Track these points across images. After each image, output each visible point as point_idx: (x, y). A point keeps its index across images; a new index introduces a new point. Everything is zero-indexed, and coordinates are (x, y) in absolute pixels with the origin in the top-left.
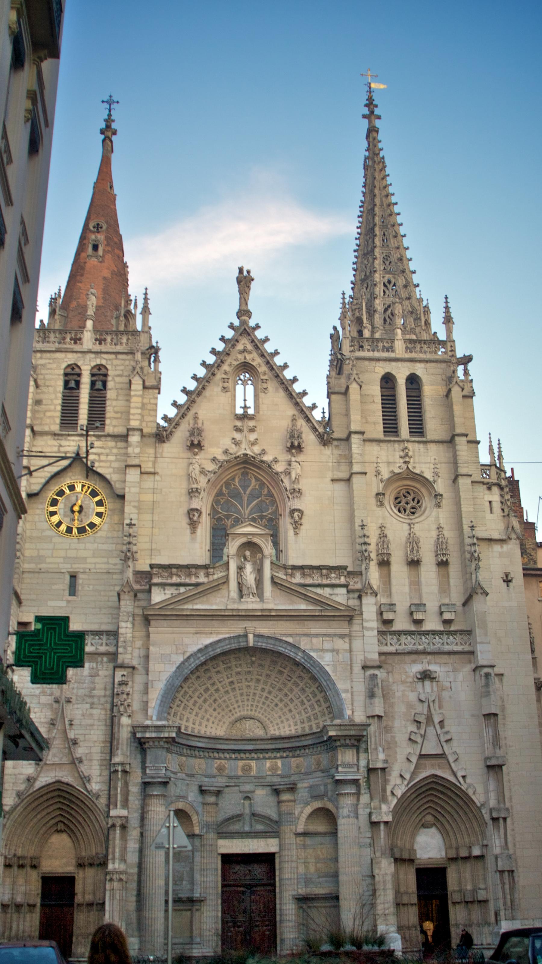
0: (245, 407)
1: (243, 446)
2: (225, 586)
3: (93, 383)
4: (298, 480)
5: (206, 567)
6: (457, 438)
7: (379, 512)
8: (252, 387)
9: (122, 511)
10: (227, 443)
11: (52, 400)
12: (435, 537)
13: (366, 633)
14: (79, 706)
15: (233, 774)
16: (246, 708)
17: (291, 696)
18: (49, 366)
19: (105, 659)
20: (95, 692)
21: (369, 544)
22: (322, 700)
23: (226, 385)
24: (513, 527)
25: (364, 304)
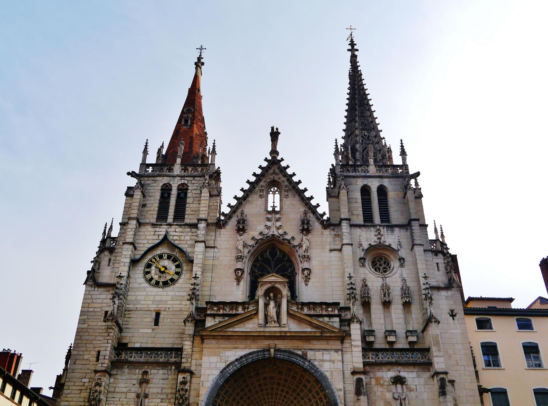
0: (274, 207)
1: (272, 230)
2: (256, 316)
3: (179, 195)
4: (307, 250)
5: (243, 304)
6: (413, 223)
7: (362, 270)
8: (279, 195)
9: (192, 271)
10: (261, 228)
11: (152, 204)
12: (401, 286)
13: (354, 349)
14: (153, 400)
17: (302, 395)
18: (152, 185)
19: (173, 367)
20: (164, 391)
21: (355, 289)
22: (323, 397)
23: (261, 194)
24: (454, 279)
25: (349, 147)
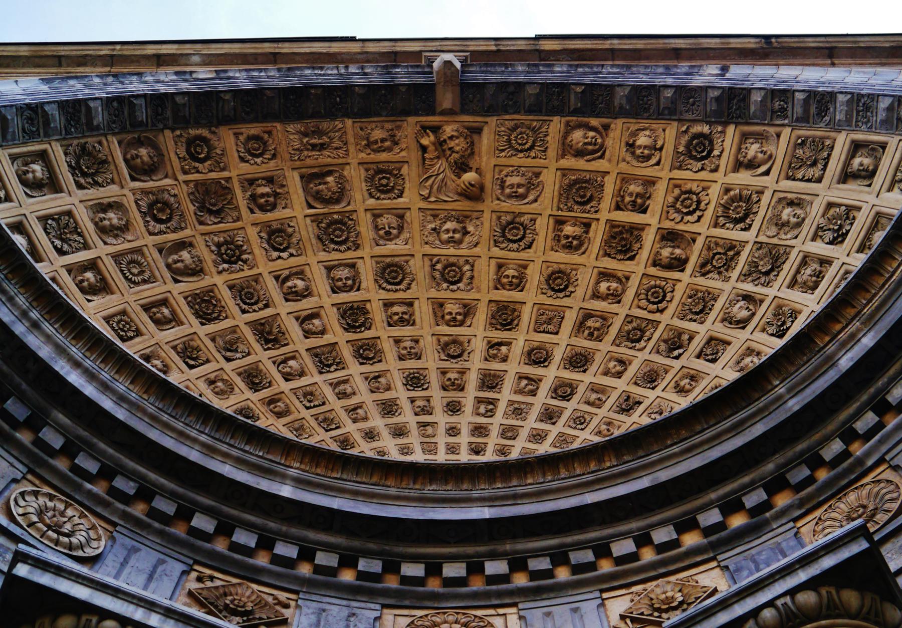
16: (442, 440)
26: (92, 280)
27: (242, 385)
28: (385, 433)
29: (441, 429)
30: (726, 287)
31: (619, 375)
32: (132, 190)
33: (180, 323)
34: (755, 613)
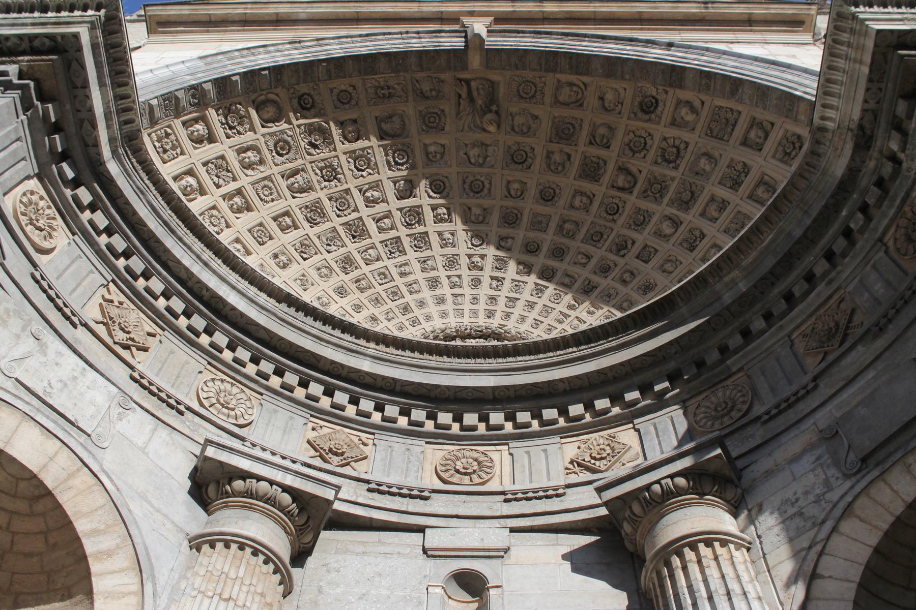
15: (394, 479)
16: (467, 307)
26: (240, 203)
27: (338, 270)
28: (430, 302)
29: (468, 298)
30: (661, 209)
31: (584, 265)
32: (263, 135)
33: (296, 228)
34: (648, 487)
